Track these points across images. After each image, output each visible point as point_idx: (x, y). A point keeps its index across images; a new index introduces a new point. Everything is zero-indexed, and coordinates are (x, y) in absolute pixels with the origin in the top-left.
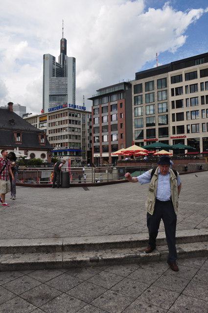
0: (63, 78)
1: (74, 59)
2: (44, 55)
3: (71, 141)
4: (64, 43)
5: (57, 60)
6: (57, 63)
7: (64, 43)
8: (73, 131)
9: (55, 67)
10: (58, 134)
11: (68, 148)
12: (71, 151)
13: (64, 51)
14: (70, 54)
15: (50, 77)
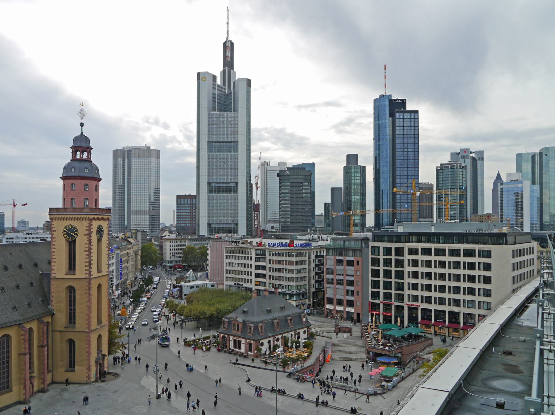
0: (231, 115)
1: (249, 82)
2: (198, 74)
3: (298, 284)
4: (229, 47)
5: (219, 82)
6: (219, 86)
7: (229, 47)
8: (300, 272)
9: (217, 92)
10: (281, 275)
11: (295, 293)
12: (297, 295)
13: (229, 63)
14: (240, 71)
15: (209, 111)
